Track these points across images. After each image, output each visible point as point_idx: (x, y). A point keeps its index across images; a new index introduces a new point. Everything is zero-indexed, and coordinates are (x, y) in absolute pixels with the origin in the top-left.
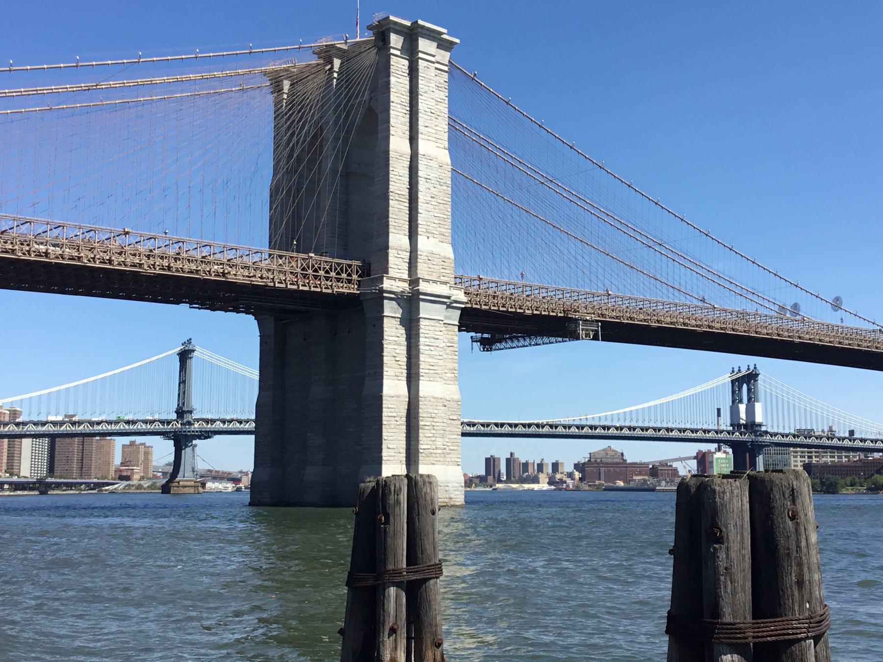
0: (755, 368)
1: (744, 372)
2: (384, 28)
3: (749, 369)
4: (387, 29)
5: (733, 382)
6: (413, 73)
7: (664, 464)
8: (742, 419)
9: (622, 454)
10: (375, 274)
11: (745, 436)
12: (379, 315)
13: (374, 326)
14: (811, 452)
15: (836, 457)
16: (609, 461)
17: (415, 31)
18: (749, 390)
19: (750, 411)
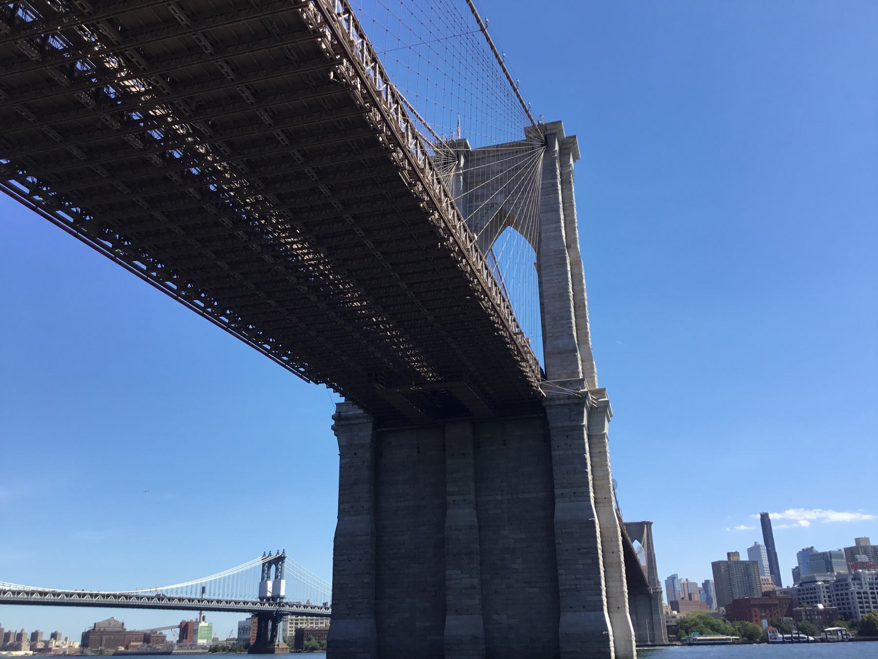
0: (284, 552)
1: (274, 556)
2: (549, 132)
3: (278, 553)
4: (551, 134)
5: (264, 564)
6: (566, 183)
7: (154, 632)
8: (270, 592)
9: (123, 624)
10: (554, 379)
11: (272, 606)
12: (574, 423)
13: (567, 436)
14: (297, 620)
15: (314, 623)
16: (111, 629)
17: (568, 146)
18: (277, 569)
19: (277, 586)
